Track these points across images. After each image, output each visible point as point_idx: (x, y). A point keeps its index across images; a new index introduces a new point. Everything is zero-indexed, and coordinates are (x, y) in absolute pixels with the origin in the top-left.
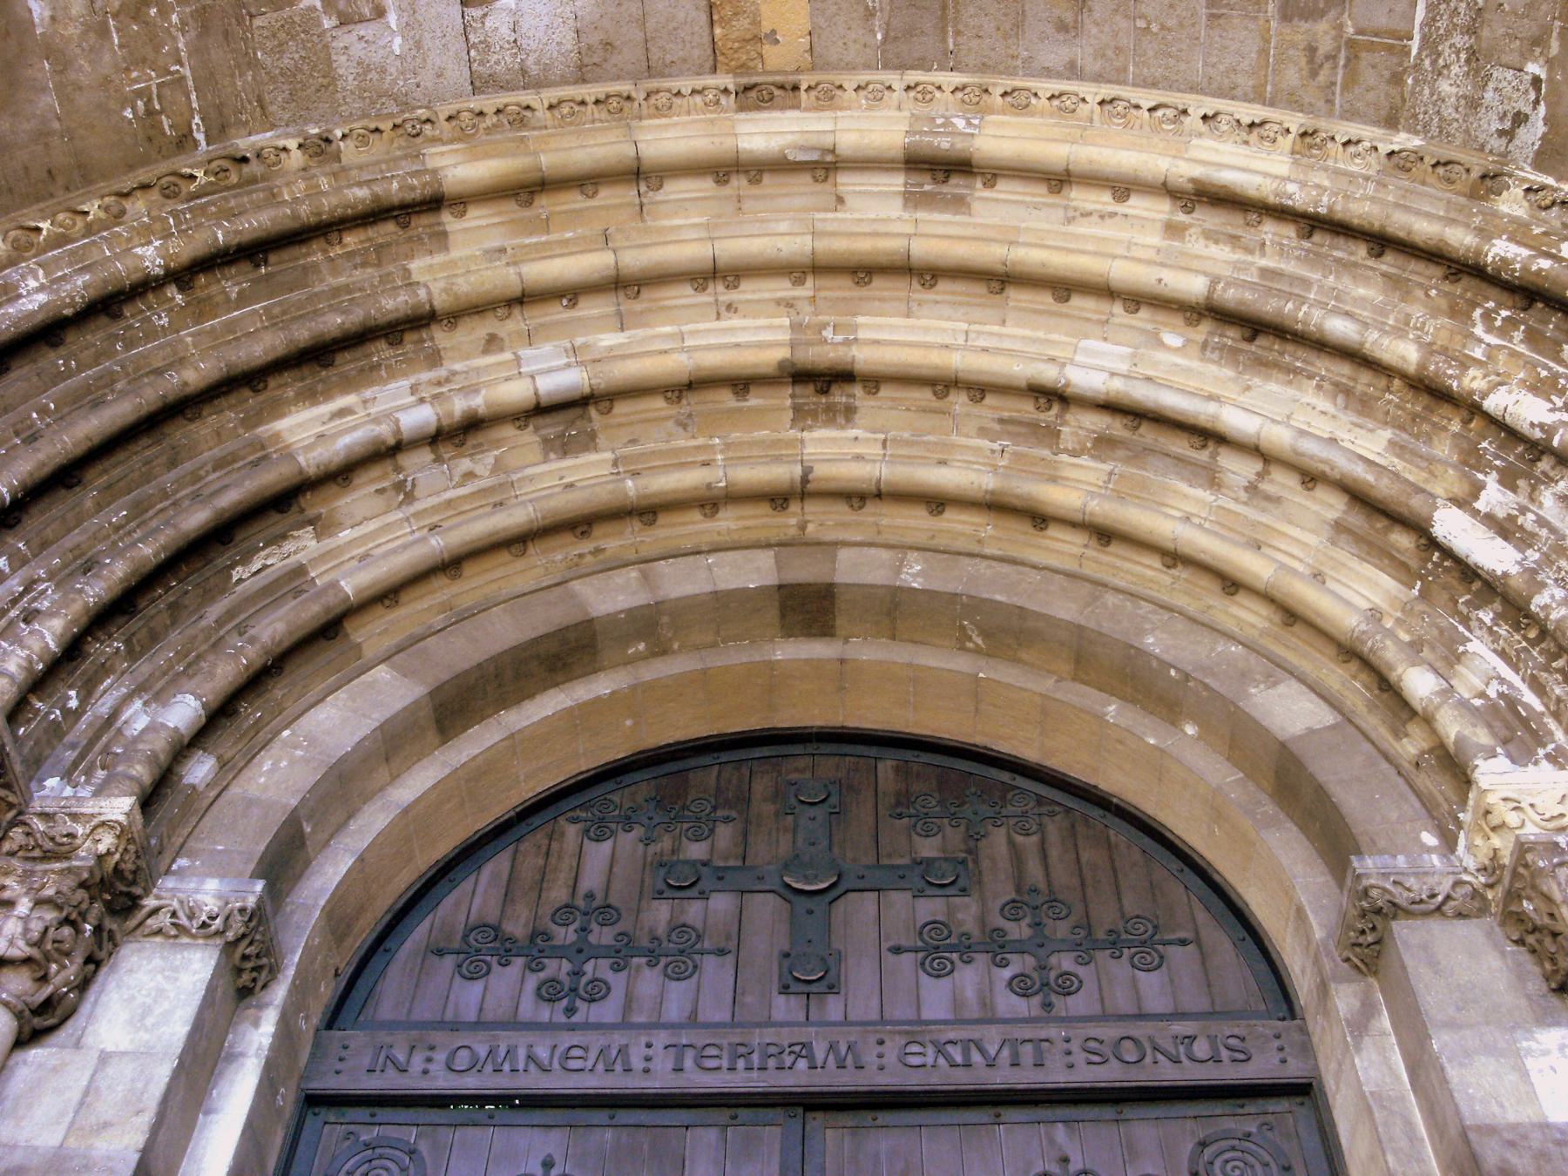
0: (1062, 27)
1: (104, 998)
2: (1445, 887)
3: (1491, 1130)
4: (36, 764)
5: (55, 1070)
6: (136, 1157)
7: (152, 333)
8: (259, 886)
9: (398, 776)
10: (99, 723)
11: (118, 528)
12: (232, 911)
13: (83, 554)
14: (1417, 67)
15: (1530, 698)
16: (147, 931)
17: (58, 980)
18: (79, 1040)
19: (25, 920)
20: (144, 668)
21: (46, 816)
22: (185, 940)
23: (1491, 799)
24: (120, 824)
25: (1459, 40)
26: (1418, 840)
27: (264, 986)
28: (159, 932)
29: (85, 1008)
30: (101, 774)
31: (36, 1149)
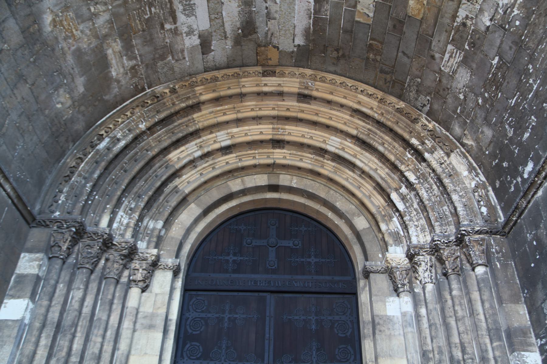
0: (334, 64)
2: (379, 269)
3: (378, 316)
5: (148, 297)
7: (144, 140)
11: (142, 186)
14: (406, 89)
15: (402, 233)
17: (147, 282)
19: (142, 274)
20: (151, 213)
21: (142, 253)
22: (166, 270)
23: (388, 259)
25: (415, 87)
26: (378, 256)
28: (161, 269)
29: (151, 284)
30: (147, 238)
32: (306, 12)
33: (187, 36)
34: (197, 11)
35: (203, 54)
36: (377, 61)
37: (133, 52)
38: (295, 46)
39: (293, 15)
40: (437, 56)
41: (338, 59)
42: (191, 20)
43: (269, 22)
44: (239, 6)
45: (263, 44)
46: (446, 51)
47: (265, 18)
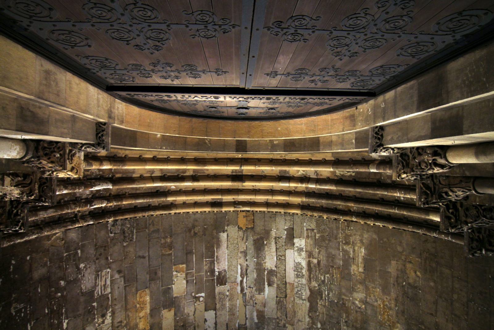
32: (220, 261)
33: (303, 248)
34: (293, 265)
35: (293, 228)
36: (163, 238)
37: (343, 255)
38: (227, 231)
39: (229, 257)
40: (117, 276)
41: (194, 227)
42: (299, 259)
43: (245, 249)
44: (265, 263)
45: (249, 230)
46: (111, 285)
47: (248, 252)
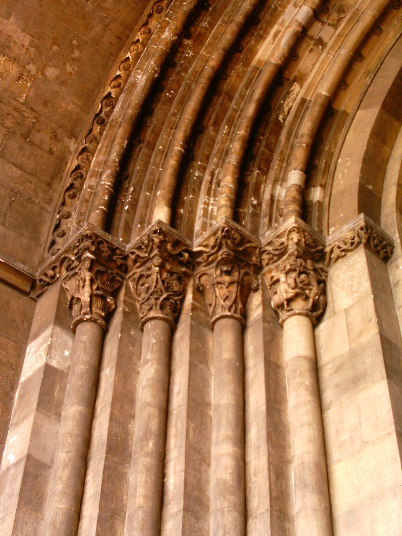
1: (334, 292)
4: (255, 231)
6: (378, 336)
7: (190, 61)
8: (362, 215)
9: (393, 146)
10: (269, 202)
11: (228, 134)
12: (358, 232)
13: (223, 151)
16: (333, 260)
17: (312, 295)
18: (334, 312)
19: (286, 282)
20: (272, 174)
21: (270, 243)
22: (349, 254)
24: (295, 227)
27: (392, 253)
29: (329, 299)
30: (281, 219)
31: (342, 355)
